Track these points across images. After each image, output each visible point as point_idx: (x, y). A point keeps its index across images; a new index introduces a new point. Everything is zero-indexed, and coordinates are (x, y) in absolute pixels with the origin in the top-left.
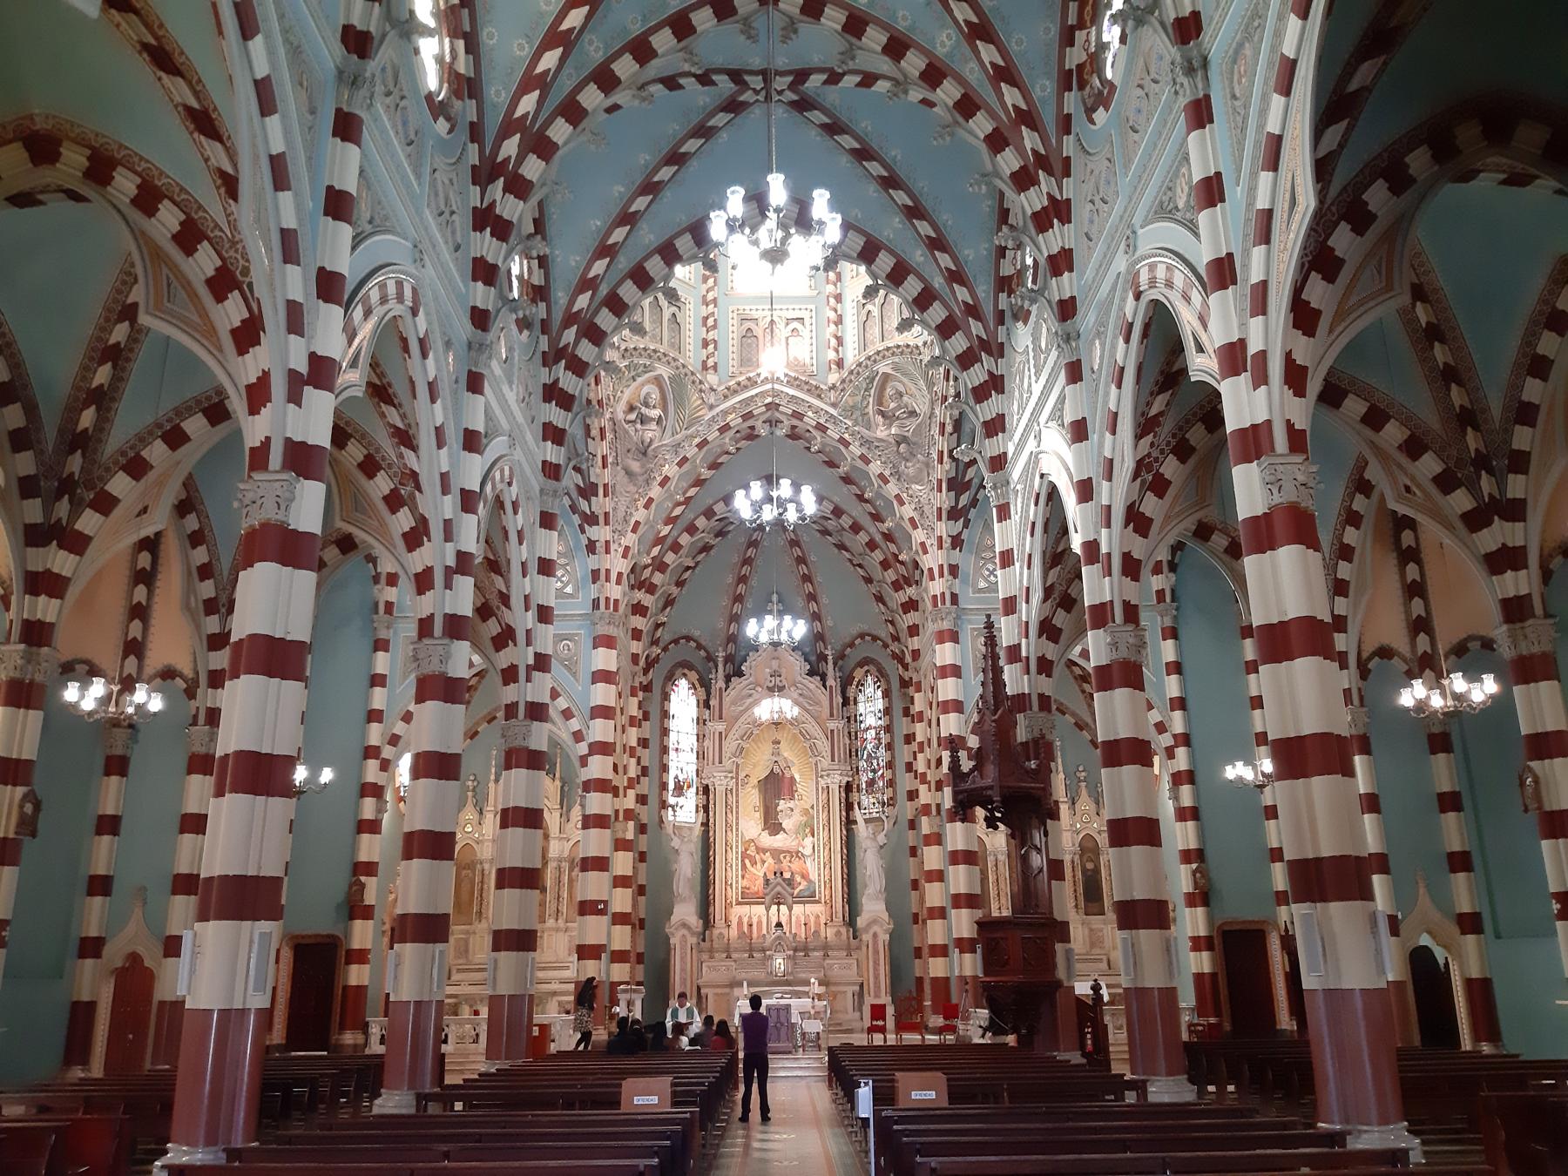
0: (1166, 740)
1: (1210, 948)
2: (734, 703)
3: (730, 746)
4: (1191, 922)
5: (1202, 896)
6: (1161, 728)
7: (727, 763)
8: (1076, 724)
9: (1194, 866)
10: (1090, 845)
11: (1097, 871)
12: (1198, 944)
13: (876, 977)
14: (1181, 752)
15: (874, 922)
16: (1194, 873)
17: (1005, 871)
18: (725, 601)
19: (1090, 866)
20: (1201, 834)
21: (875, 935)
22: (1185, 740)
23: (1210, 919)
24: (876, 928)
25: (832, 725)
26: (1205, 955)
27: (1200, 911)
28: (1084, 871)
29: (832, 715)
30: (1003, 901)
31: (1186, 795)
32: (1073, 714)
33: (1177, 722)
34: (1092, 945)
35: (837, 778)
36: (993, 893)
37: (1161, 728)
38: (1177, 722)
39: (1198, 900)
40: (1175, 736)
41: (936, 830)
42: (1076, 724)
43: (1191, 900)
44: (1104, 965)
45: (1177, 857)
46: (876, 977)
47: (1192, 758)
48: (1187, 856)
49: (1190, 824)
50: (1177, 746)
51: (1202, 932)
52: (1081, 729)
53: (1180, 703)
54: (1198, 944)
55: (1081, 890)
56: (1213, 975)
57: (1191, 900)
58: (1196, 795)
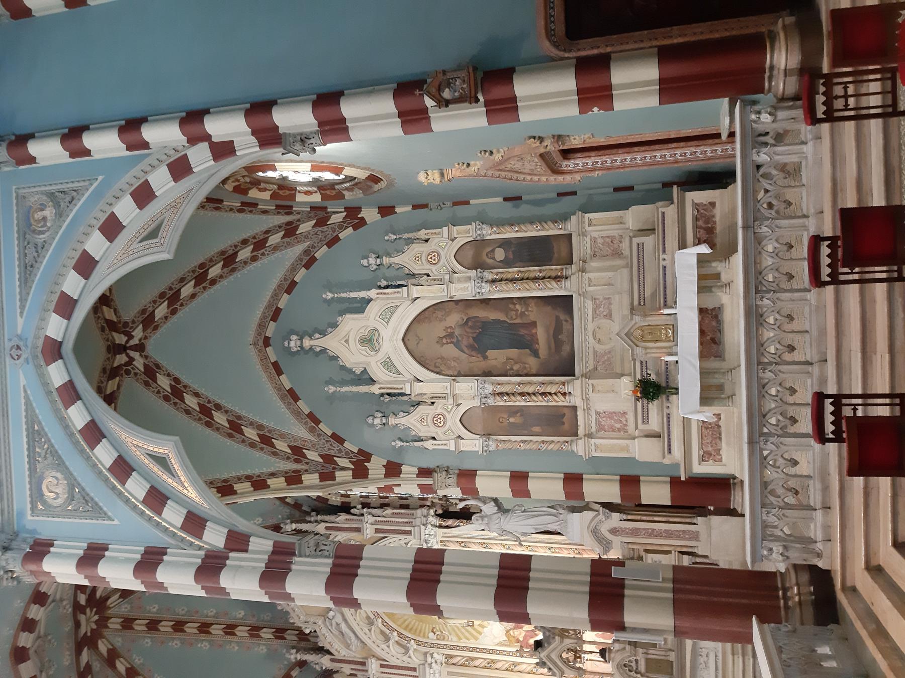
0: (200, 157)
1: (602, 63)
2: (348, 646)
3: (393, 654)
4: (547, 98)
5: (490, 81)
6: (180, 168)
7: (415, 660)
8: (307, 266)
9: (429, 102)
10: (469, 253)
11: (505, 244)
12: (595, 94)
13: (669, 535)
14: (219, 127)
15: (595, 533)
16: (444, 103)
17: (511, 383)
18: (233, 646)
19: (500, 254)
20: (367, 86)
21: (613, 531)
22: (192, 119)
23: (542, 64)
24: (604, 530)
25: (369, 531)
26: (620, 75)
27: (522, 88)
28: (507, 263)
29: (358, 530)
30: (552, 389)
31: (294, 118)
32: (294, 269)
33: (164, 135)
34: (617, 254)
35: (430, 530)
36: (541, 402)
37: (180, 168)
38: (164, 135)
39: (498, 92)
40: (193, 141)
41: (453, 480)
42: (307, 266)
43: (503, 108)
44: (649, 241)
45: (418, 139)
46: (669, 535)
47: (225, 106)
48: (413, 119)
49: (349, 109)
50: (207, 137)
51: (567, 83)
52: (313, 260)
53: (130, 128)
54: (595, 94)
55: (535, 271)
56: (665, 55)
57: (503, 108)
58: (292, 98)
